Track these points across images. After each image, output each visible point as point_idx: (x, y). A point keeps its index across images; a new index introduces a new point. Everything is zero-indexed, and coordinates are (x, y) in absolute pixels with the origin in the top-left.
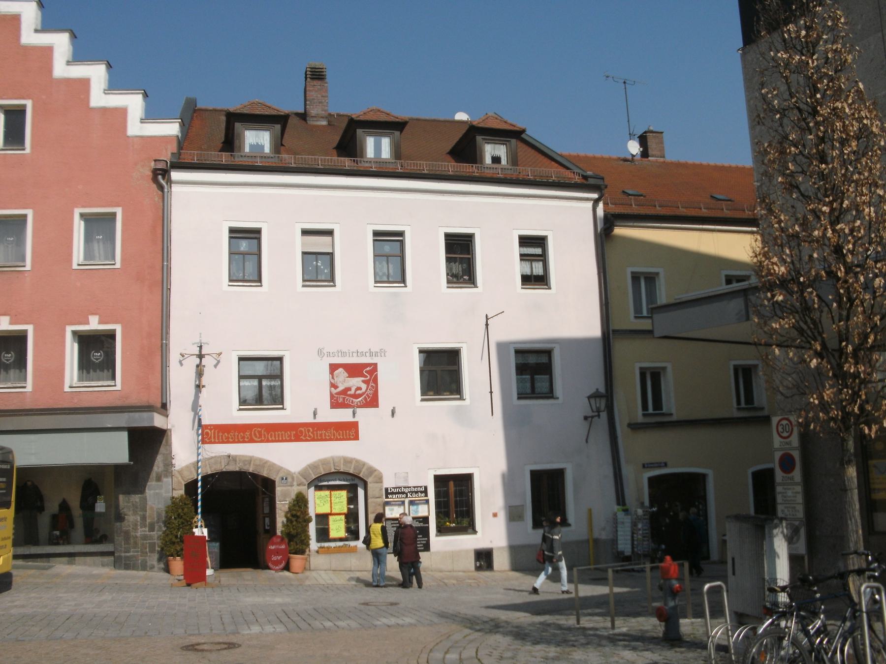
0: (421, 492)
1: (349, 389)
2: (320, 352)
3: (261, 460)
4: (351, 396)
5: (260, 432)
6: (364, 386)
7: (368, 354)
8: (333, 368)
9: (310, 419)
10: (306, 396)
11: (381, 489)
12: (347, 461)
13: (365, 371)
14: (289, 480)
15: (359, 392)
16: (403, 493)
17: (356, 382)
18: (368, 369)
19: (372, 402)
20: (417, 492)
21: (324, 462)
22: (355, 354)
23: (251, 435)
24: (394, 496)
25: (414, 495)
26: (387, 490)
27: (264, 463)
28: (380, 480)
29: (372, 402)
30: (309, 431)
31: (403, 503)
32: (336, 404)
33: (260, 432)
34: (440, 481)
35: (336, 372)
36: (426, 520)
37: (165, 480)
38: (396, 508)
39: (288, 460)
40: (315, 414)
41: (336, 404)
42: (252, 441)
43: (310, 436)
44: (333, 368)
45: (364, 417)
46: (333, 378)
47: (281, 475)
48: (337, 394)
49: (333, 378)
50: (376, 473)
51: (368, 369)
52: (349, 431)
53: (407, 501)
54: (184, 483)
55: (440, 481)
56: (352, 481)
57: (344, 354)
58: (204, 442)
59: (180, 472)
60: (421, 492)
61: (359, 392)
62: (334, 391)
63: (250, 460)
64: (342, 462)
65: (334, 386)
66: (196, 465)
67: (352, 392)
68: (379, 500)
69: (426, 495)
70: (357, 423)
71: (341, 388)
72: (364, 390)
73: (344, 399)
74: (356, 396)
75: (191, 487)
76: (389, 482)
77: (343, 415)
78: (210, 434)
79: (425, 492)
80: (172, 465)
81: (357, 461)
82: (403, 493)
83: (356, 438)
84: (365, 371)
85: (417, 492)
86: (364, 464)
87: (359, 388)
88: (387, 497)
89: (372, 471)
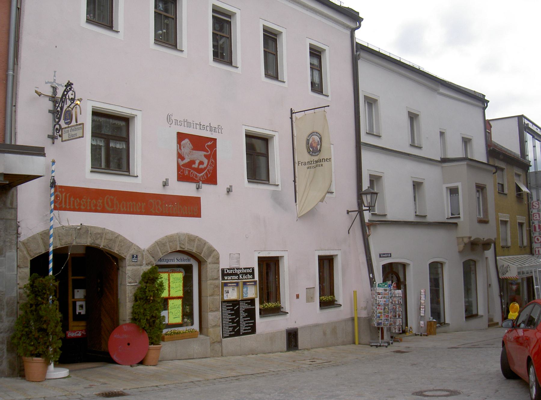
0: (250, 274)
1: (193, 162)
2: (169, 118)
3: (113, 233)
4: (195, 169)
5: (112, 201)
6: (206, 161)
7: (208, 128)
8: (181, 137)
9: (157, 190)
10: (152, 166)
11: (219, 271)
12: (192, 239)
13: (206, 145)
14: (140, 258)
15: (201, 166)
16: (236, 274)
17: (199, 156)
18: (209, 143)
19: (212, 179)
20: (246, 274)
21: (171, 239)
22: (198, 127)
23: (103, 203)
24: (230, 278)
25: (245, 277)
26: (223, 270)
27: (116, 238)
28: (217, 261)
29: (212, 179)
30: (158, 204)
31: (237, 284)
32: (182, 177)
33: (112, 201)
34: (261, 260)
35: (183, 142)
36: (252, 302)
37: (8, 254)
38: (230, 289)
39: (139, 234)
40: (165, 184)
41: (182, 177)
42: (103, 211)
43: (158, 209)
44: (181, 137)
45: (207, 194)
46: (180, 148)
47: (132, 252)
48: (183, 165)
49: (180, 148)
50: (214, 253)
51: (209, 143)
52: (190, 207)
53: (241, 284)
54: (30, 259)
55: (261, 260)
56: (190, 260)
57: (189, 125)
58: (55, 208)
59: (24, 243)
60: (250, 274)
61: (201, 166)
62: (182, 163)
63: (102, 233)
64: (187, 239)
65: (180, 156)
66: (45, 235)
67: (196, 166)
68: (217, 282)
69: (253, 278)
70: (199, 199)
71: (187, 160)
72: (205, 165)
73: (189, 171)
74: (200, 171)
75: (38, 264)
76: (224, 264)
77: (187, 189)
78: (69, 198)
79: (252, 273)
80: (18, 234)
81: (200, 240)
82: (236, 274)
83: (198, 215)
84: (206, 145)
85: (246, 274)
86: (205, 243)
87: (201, 163)
88: (223, 279)
89: (211, 250)
